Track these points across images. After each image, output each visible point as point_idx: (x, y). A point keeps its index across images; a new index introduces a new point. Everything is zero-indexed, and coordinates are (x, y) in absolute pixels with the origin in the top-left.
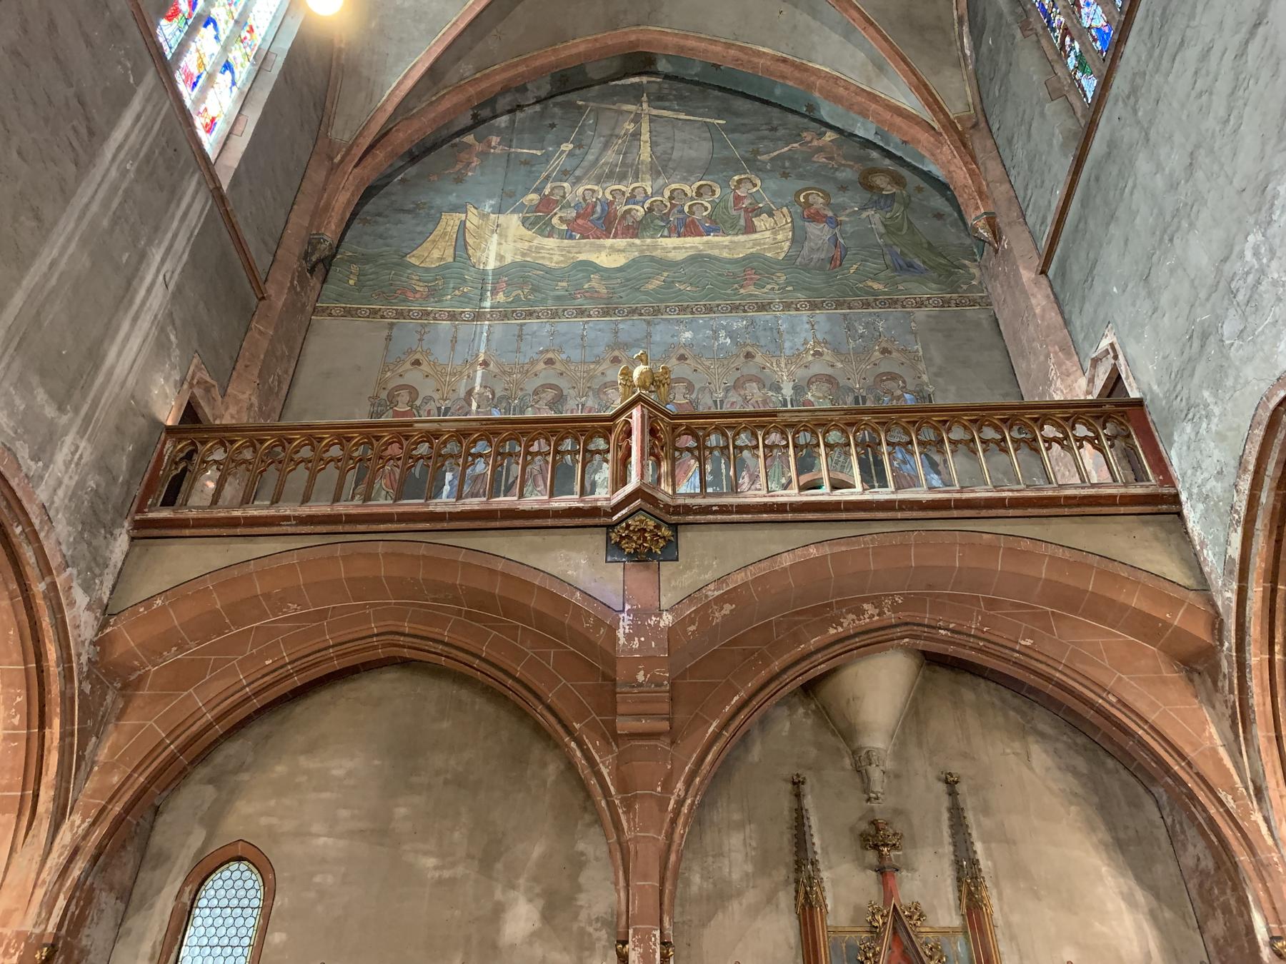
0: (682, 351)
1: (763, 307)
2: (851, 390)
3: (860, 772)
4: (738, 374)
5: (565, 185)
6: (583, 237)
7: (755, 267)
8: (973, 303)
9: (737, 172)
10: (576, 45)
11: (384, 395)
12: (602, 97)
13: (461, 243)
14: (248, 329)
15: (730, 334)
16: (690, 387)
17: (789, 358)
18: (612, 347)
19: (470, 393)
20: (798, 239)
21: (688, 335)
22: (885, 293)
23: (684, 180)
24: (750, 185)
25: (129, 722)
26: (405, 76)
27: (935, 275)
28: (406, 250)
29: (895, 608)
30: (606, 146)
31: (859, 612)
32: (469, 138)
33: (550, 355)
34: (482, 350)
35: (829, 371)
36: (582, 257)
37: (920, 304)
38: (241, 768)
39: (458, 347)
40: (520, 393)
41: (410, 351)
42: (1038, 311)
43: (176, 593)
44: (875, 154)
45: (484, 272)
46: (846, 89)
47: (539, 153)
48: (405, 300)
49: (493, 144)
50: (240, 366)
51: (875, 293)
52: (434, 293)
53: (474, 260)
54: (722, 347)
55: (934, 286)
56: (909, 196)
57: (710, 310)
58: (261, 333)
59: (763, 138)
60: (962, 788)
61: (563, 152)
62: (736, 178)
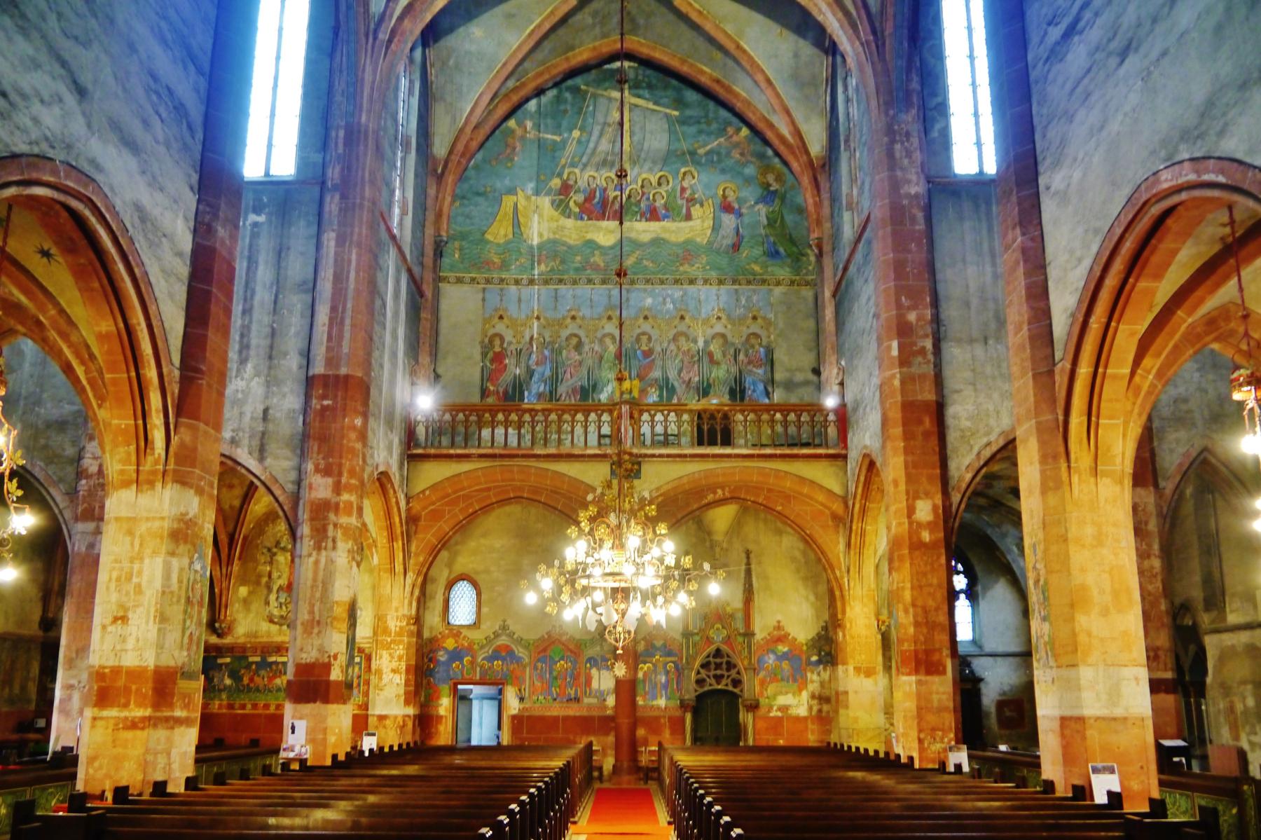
0: (646, 313)
1: (692, 282)
2: (733, 344)
3: (712, 547)
4: (675, 331)
5: (577, 171)
6: (590, 219)
7: (688, 252)
8: (807, 283)
9: (685, 164)
10: (581, 53)
11: (486, 340)
12: (599, 83)
13: (516, 224)
14: (419, 319)
15: (673, 303)
16: (650, 339)
17: (703, 320)
18: (607, 309)
19: (532, 338)
20: (716, 227)
21: (649, 301)
22: (761, 275)
23: (651, 170)
24: (691, 178)
25: (420, 536)
26: (476, 103)
27: (789, 261)
28: (485, 229)
29: (730, 492)
30: (601, 134)
31: (715, 493)
32: (512, 123)
33: (573, 313)
34: (536, 308)
35: (722, 330)
36: (589, 236)
37: (778, 283)
38: (457, 543)
39: (523, 306)
40: (559, 340)
41: (496, 310)
42: (827, 318)
43: (434, 487)
44: (770, 152)
45: (531, 247)
46: (754, 114)
47: (557, 138)
48: (489, 270)
49: (528, 128)
50: (421, 341)
51: (754, 274)
52: (504, 266)
53: (525, 236)
54: (668, 311)
55: (788, 269)
56: (785, 192)
57: (662, 282)
58: (426, 319)
59: (700, 132)
60: (752, 556)
61: (574, 139)
62: (683, 170)
